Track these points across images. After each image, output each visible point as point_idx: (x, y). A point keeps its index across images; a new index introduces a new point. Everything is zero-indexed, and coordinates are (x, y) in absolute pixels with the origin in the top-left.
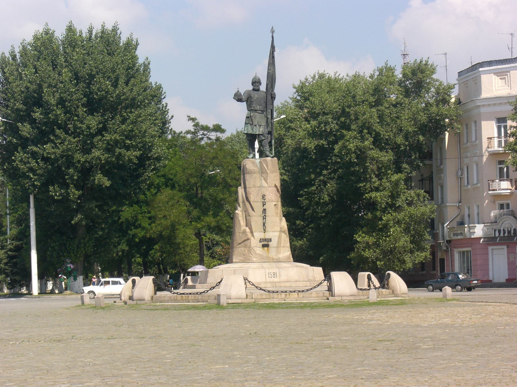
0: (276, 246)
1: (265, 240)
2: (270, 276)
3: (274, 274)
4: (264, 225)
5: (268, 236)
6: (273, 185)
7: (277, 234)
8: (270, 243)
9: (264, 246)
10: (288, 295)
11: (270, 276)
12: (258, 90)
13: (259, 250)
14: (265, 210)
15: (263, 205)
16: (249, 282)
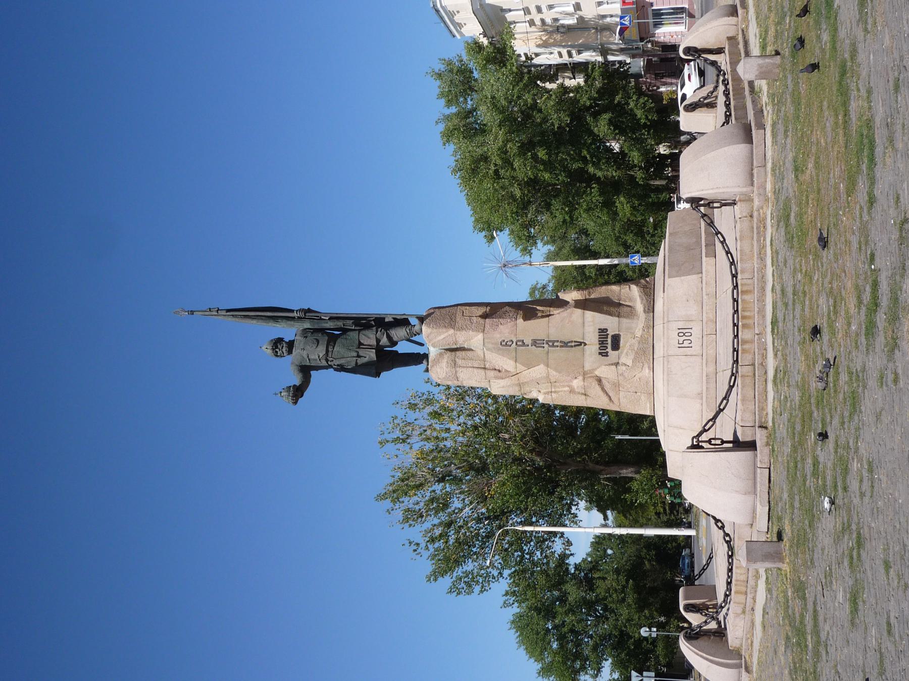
0: (617, 319)
1: (602, 343)
2: (686, 344)
3: (683, 333)
4: (565, 344)
5: (592, 339)
6: (481, 321)
7: (589, 314)
8: (611, 333)
9: (616, 346)
10: (745, 321)
11: (686, 344)
12: (291, 345)
13: (626, 355)
14: (535, 343)
15: (524, 344)
16: (704, 431)
